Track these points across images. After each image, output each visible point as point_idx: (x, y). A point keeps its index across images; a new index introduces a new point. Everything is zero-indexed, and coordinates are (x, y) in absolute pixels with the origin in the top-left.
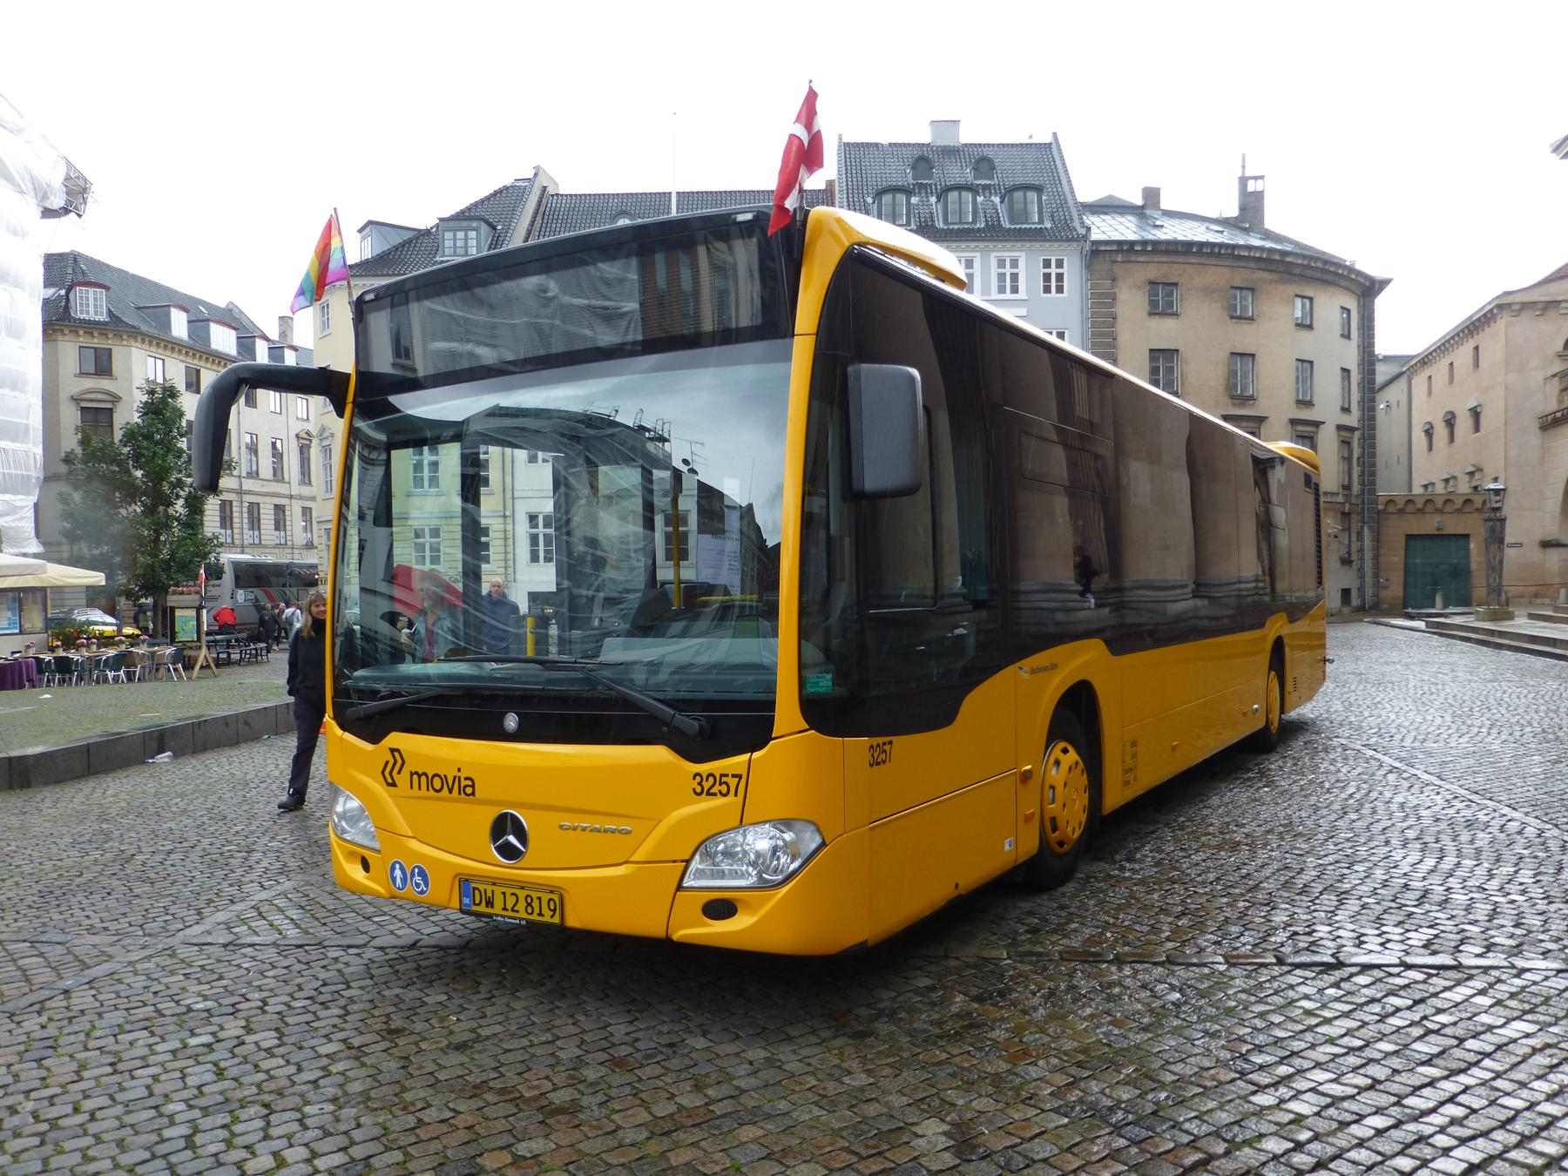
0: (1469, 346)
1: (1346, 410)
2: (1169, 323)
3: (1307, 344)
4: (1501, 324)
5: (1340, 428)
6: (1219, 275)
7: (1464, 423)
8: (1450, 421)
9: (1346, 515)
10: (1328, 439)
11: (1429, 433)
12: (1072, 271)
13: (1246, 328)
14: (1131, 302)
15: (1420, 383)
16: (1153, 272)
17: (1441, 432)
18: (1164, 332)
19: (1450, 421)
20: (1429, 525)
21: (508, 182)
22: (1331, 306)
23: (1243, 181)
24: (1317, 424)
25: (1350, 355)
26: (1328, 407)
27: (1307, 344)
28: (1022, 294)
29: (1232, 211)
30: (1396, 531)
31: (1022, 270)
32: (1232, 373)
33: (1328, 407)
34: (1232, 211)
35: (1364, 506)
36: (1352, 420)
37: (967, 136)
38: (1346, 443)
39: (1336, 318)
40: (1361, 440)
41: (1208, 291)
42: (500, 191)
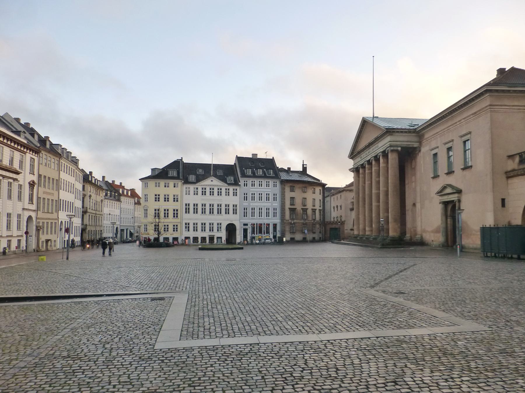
0: (339, 195)
1: (320, 207)
2: (293, 193)
3: (314, 196)
4: (345, 192)
5: (320, 210)
6: (301, 185)
7: (339, 208)
8: (337, 207)
9: (320, 225)
10: (317, 212)
11: (334, 208)
12: (278, 184)
13: (305, 194)
14: (287, 189)
15: (332, 198)
16: (291, 184)
17: (336, 208)
18: (293, 194)
19: (337, 207)
20: (334, 226)
21: (176, 159)
22: (318, 189)
23: (303, 165)
24: (316, 209)
25: (321, 197)
26: (317, 207)
27: (314, 196)
28: (270, 187)
29: (301, 170)
30: (329, 227)
31: (270, 183)
32: (303, 201)
33: (317, 207)
34: (301, 170)
35: (324, 223)
36: (321, 208)
37: (258, 157)
38: (320, 212)
39: (319, 191)
40: (323, 211)
41: (299, 188)
42: (175, 162)
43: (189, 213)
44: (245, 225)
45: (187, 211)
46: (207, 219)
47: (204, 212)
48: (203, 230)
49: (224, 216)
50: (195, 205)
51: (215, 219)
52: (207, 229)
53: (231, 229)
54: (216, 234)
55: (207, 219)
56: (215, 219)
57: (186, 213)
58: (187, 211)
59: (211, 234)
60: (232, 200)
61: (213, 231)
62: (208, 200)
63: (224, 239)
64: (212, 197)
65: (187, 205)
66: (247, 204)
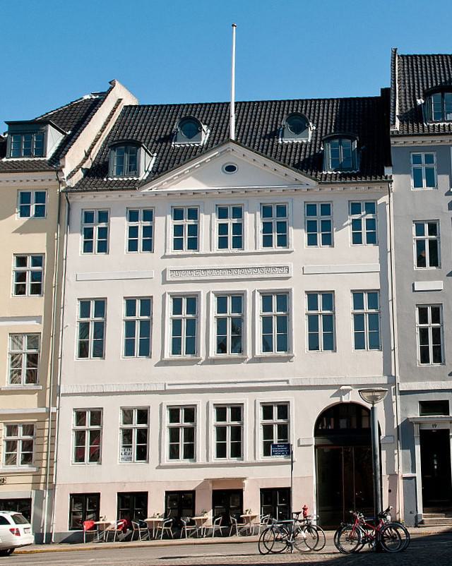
43: (99, 352)
44: (427, 407)
45: (93, 345)
46: (206, 381)
47: (185, 340)
48: (182, 444)
49: (304, 362)
50: (140, 306)
51: (250, 379)
52: (205, 439)
53: (345, 432)
54: (255, 474)
55: (206, 381)
56: (250, 379)
57: (83, 353)
58: (93, 345)
59: (226, 471)
60: (345, 265)
61: (237, 452)
62: (210, 269)
63: (305, 499)
64: (232, 260)
65: (95, 308)
66: (438, 285)
